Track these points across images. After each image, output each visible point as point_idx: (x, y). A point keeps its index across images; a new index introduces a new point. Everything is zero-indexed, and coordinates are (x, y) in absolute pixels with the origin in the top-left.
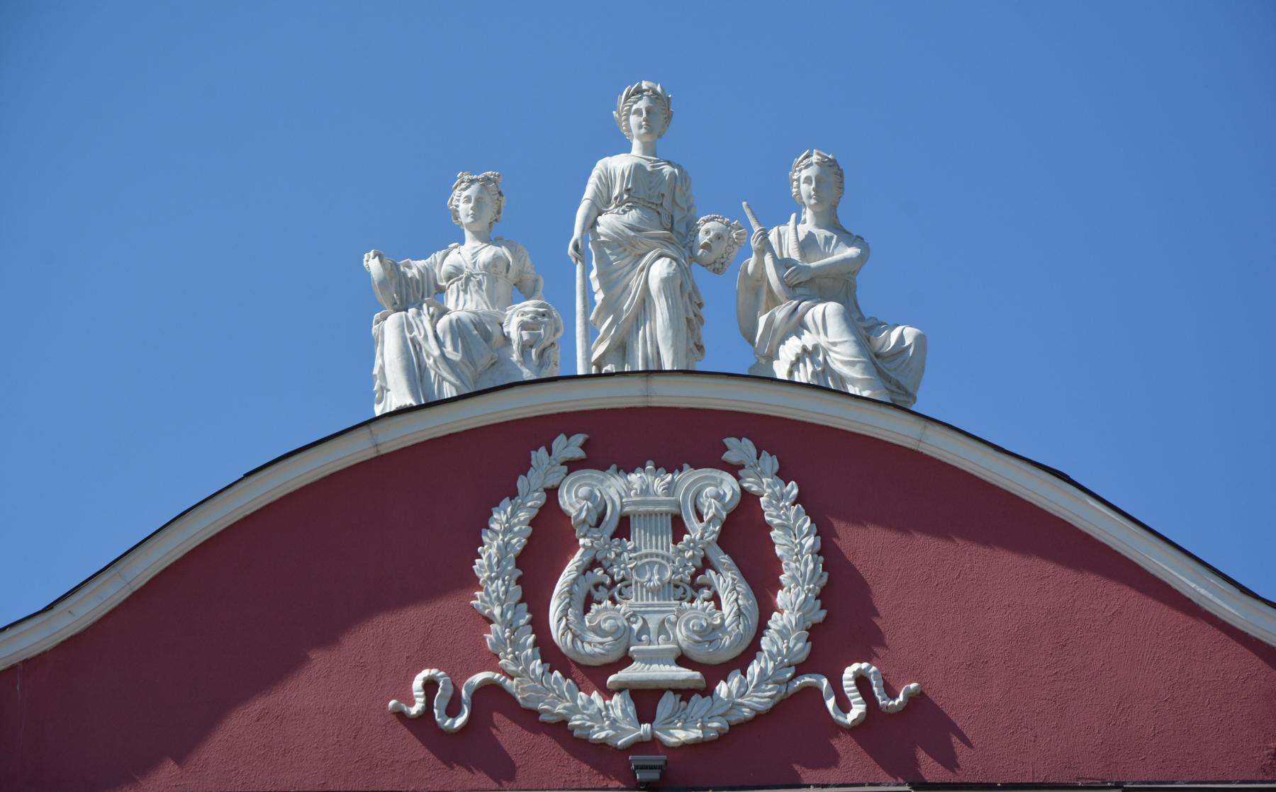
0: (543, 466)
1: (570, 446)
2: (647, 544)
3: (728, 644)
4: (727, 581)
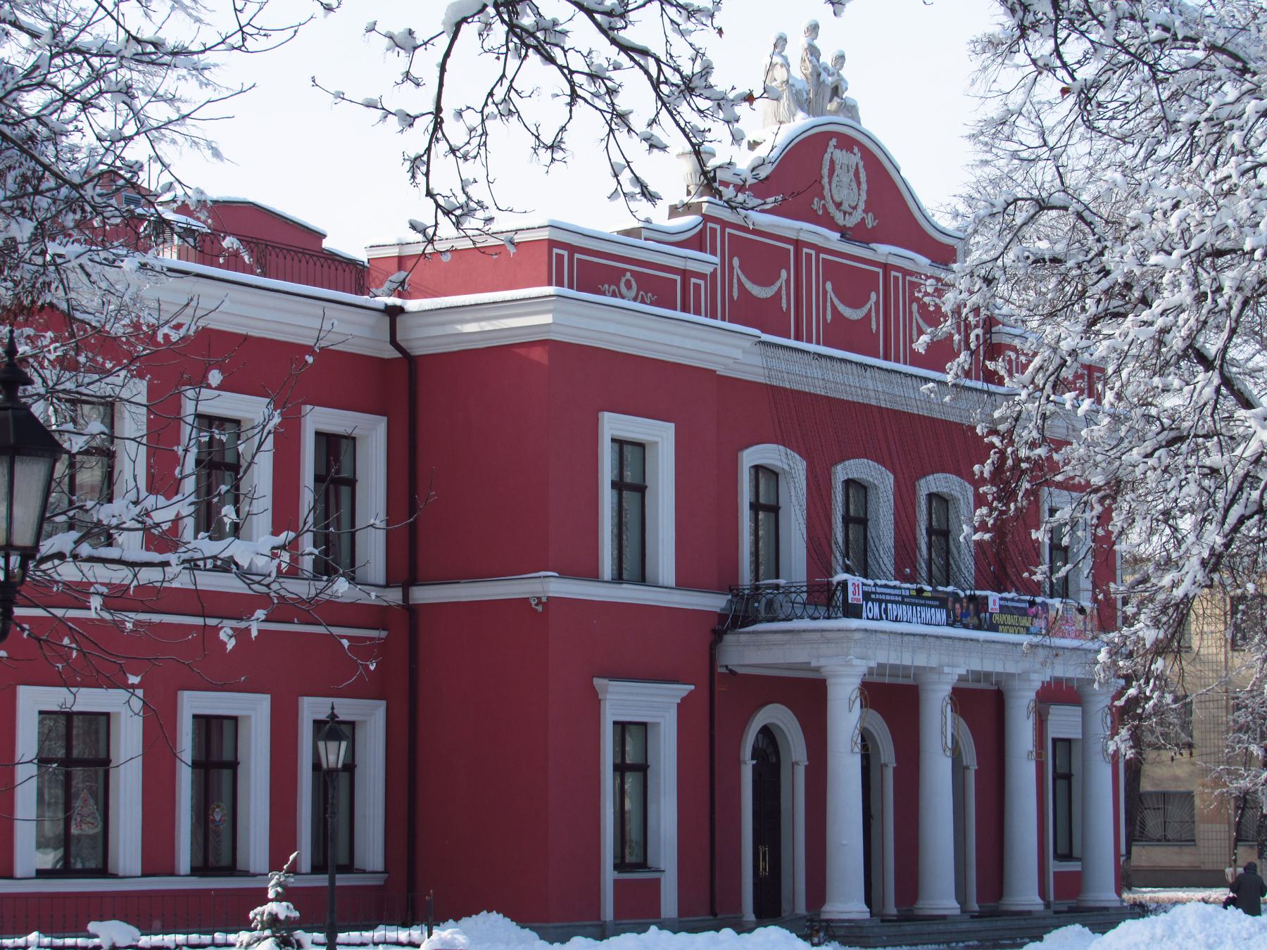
1: (833, 142)
4: (854, 185)
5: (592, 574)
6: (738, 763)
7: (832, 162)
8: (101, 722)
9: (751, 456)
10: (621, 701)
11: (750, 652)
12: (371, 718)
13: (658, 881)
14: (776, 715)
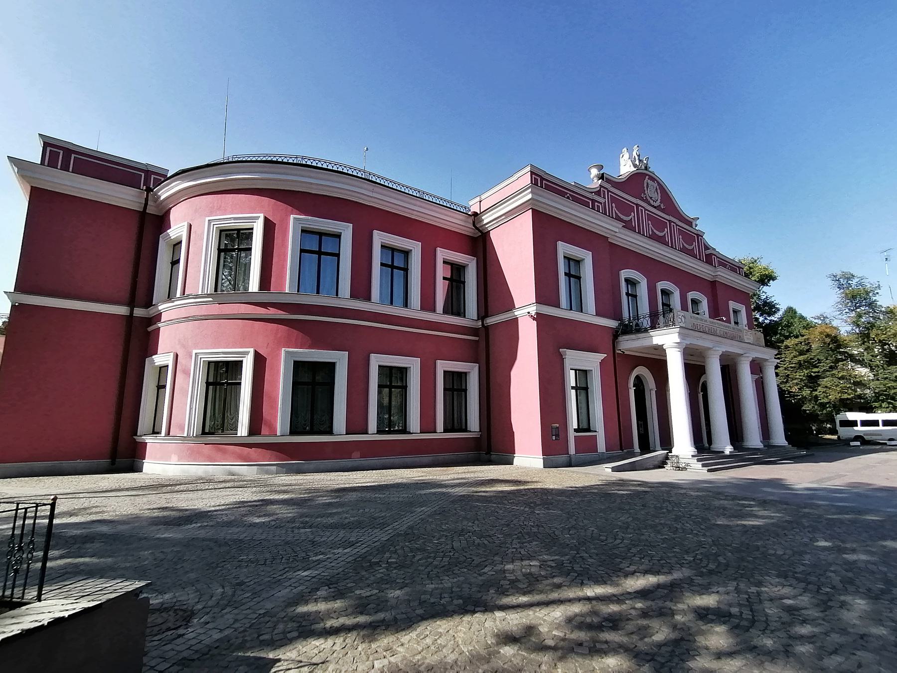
5: (557, 305)
6: (628, 389)
8: (330, 367)
9: (625, 274)
11: (629, 344)
12: (473, 373)
14: (641, 370)
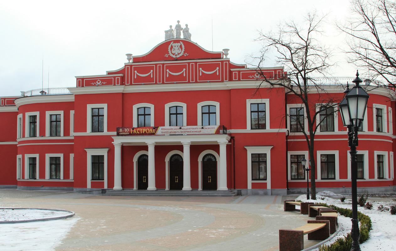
0: (172, 43)
1: (173, 42)
2: (176, 47)
3: (180, 52)
4: (180, 49)
7: (172, 47)
10: (91, 153)
13: (104, 182)
